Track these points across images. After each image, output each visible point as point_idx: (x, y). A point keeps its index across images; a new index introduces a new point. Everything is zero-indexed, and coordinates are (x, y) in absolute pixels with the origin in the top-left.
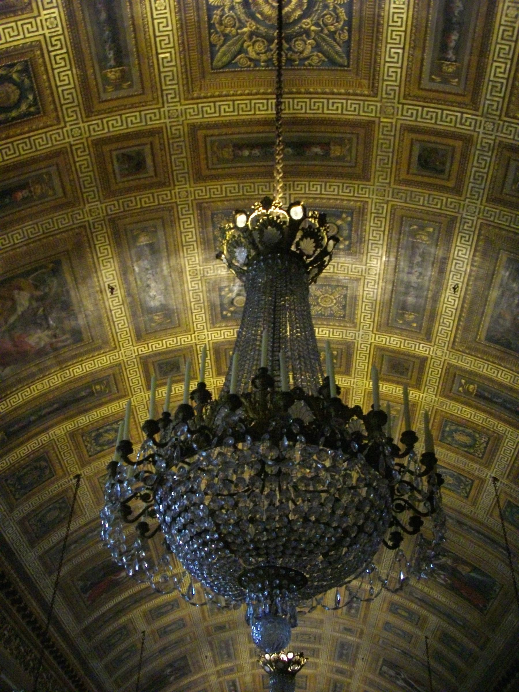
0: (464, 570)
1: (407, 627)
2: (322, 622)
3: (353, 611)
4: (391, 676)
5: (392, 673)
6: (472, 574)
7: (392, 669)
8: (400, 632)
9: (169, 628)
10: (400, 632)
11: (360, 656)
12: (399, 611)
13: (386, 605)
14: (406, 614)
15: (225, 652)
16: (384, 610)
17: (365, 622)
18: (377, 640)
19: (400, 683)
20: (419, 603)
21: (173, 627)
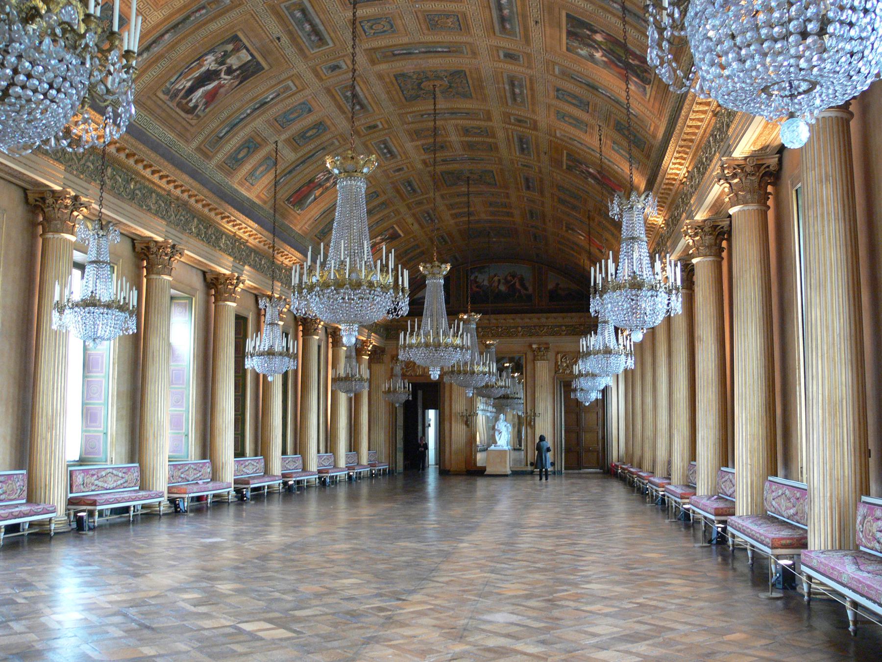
0: (317, 192)
1: (296, 128)
2: (373, 62)
3: (349, 94)
4: (226, 55)
5: (233, 62)
6: (313, 196)
7: (240, 68)
8: (292, 116)
9: (574, 101)
10: (292, 116)
11: (285, 39)
12: (315, 131)
13: (329, 123)
14: (308, 134)
15: (506, 12)
16: (327, 120)
17: (328, 91)
18: (297, 83)
19: (210, 62)
20: (313, 152)
21: (570, 99)
